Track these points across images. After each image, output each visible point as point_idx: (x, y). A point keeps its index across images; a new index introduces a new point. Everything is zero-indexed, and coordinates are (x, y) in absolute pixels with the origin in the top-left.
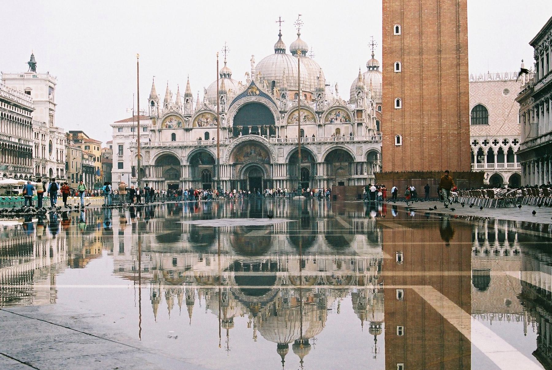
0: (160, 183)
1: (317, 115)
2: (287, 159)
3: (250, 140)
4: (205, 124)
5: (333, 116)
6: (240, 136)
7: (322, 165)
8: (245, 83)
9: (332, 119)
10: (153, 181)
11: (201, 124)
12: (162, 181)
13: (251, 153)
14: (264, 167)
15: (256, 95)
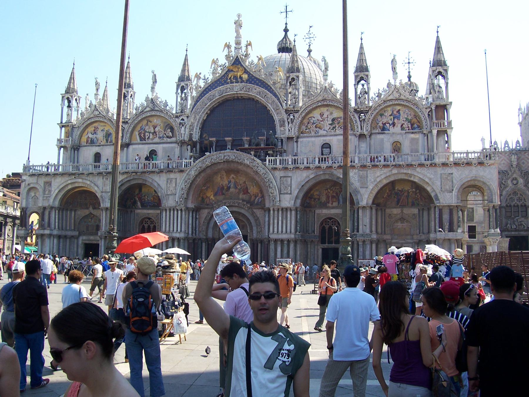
0: (68, 240)
1: (356, 116)
2: (297, 197)
3: (227, 162)
4: (151, 136)
5: (387, 118)
6: (207, 154)
7: (368, 212)
8: (223, 61)
9: (384, 124)
10: (54, 236)
11: (144, 135)
12: (72, 236)
13: (229, 188)
14: (253, 214)
15: (242, 81)
